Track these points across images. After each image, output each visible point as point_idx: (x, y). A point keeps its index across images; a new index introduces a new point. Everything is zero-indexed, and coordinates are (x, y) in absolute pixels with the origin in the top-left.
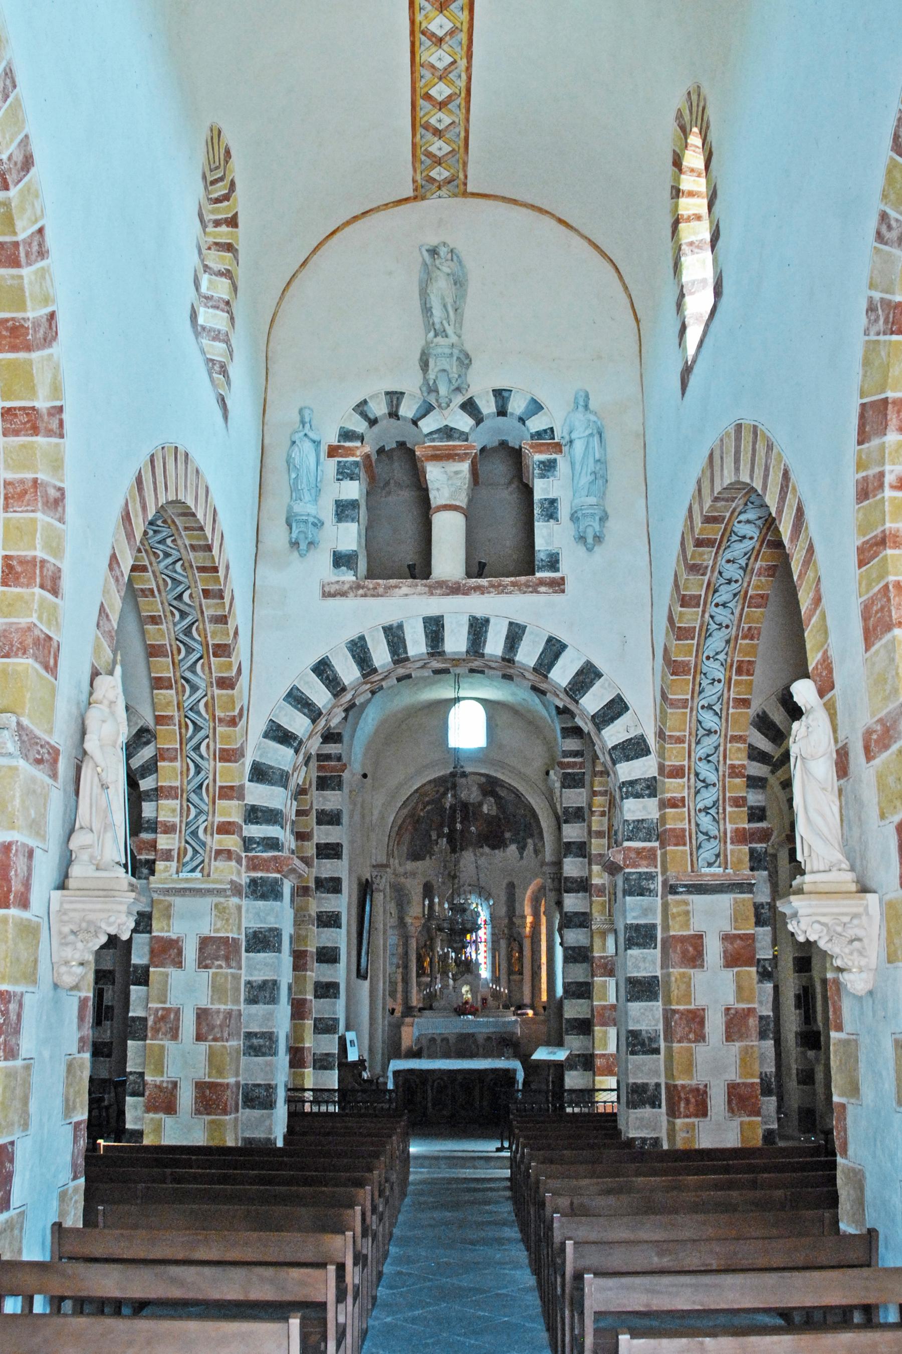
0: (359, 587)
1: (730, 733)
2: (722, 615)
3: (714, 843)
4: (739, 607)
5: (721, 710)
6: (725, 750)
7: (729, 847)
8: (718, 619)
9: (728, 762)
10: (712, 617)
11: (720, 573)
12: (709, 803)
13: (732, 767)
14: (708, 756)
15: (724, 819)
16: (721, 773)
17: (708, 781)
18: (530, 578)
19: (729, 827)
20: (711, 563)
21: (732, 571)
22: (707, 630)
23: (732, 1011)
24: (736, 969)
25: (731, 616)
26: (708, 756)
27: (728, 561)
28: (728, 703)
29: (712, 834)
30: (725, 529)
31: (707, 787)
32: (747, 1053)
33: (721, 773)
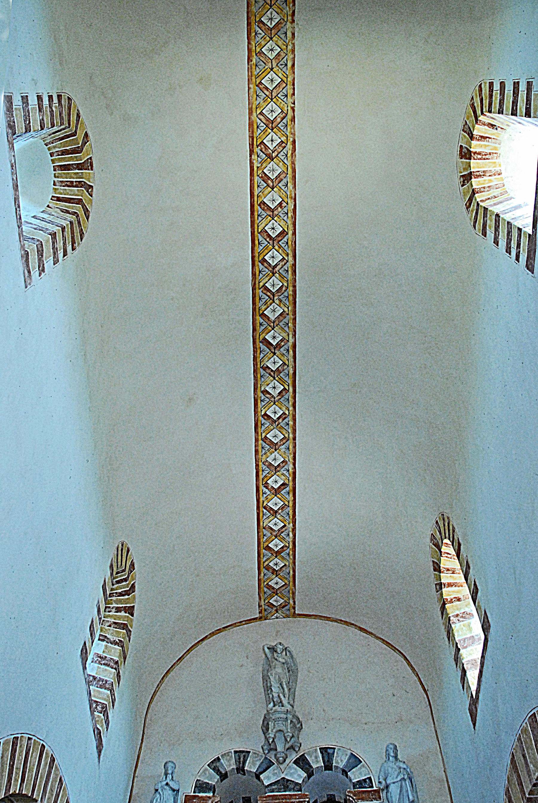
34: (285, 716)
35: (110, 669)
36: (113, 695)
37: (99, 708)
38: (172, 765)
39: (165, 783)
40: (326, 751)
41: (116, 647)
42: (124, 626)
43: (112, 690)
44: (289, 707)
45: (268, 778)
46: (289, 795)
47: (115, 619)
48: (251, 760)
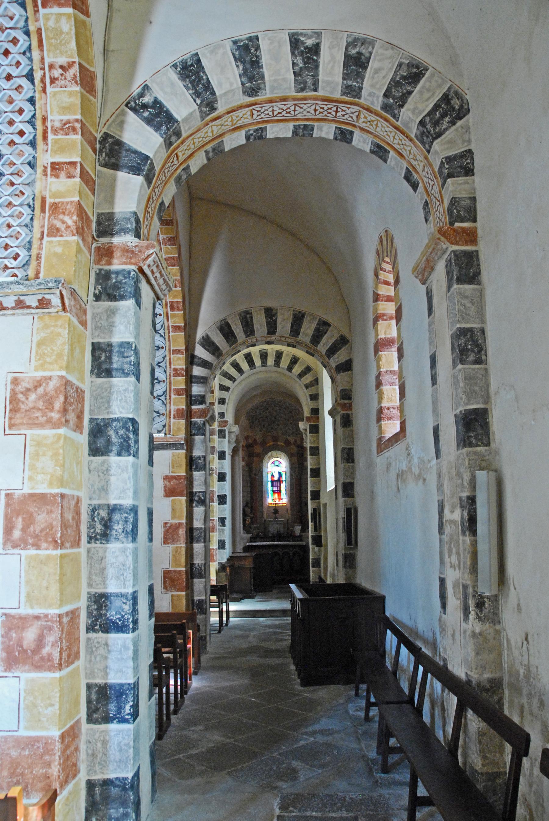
1: (172, 348)
3: (162, 418)
5: (164, 333)
6: (170, 359)
7: (172, 420)
9: (172, 367)
12: (160, 393)
13: (175, 370)
14: (159, 363)
15: (170, 403)
16: (168, 374)
17: (160, 379)
19: (173, 408)
23: (168, 525)
24: (172, 498)
26: (159, 363)
28: (169, 329)
29: (161, 412)
31: (159, 382)
32: (177, 551)
33: (168, 374)
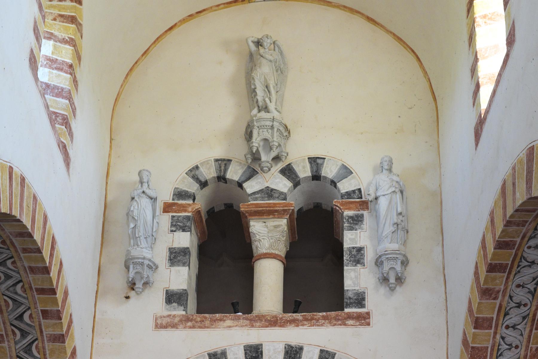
0: (188, 319)
2: (512, 336)
4: (528, 330)
8: (509, 340)
10: (503, 338)
11: (511, 297)
18: (340, 313)
20: (502, 287)
21: (521, 295)
22: (499, 350)
25: (520, 338)
27: (518, 286)
30: (516, 255)
34: (271, 124)
35: (65, 74)
36: (72, 104)
37: (59, 119)
38: (147, 173)
39: (142, 191)
40: (315, 162)
41: (67, 46)
42: (73, 20)
43: (70, 98)
44: (276, 114)
45: (251, 187)
46: (274, 204)
47: (59, 11)
48: (233, 169)
